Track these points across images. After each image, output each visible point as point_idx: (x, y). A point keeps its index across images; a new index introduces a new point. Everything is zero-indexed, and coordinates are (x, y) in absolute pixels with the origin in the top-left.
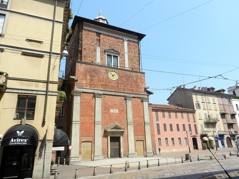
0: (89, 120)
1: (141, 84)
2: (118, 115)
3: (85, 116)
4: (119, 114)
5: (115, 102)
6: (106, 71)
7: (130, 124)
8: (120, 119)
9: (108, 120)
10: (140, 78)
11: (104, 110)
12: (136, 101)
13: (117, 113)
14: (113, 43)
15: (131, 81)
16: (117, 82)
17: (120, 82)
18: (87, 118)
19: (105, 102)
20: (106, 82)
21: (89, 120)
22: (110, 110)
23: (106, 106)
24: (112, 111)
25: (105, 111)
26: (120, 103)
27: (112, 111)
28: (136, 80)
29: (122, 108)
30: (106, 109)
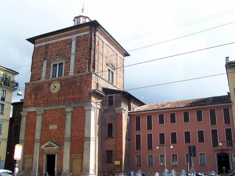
0: (31, 139)
1: (86, 88)
2: (56, 131)
3: (28, 134)
4: (57, 129)
5: (55, 117)
6: (48, 84)
7: (67, 140)
8: (58, 135)
9: (46, 137)
10: (86, 81)
11: (44, 127)
12: (78, 112)
13: (56, 129)
14: (60, 49)
15: (74, 88)
16: (59, 94)
17: (61, 93)
18: (30, 136)
19: (46, 118)
20: (47, 97)
21: (31, 139)
22: (49, 126)
23: (46, 122)
24: (51, 127)
25: (45, 129)
26: (59, 117)
27: (51, 127)
28: (80, 84)
29: (61, 123)
30: (45, 125)
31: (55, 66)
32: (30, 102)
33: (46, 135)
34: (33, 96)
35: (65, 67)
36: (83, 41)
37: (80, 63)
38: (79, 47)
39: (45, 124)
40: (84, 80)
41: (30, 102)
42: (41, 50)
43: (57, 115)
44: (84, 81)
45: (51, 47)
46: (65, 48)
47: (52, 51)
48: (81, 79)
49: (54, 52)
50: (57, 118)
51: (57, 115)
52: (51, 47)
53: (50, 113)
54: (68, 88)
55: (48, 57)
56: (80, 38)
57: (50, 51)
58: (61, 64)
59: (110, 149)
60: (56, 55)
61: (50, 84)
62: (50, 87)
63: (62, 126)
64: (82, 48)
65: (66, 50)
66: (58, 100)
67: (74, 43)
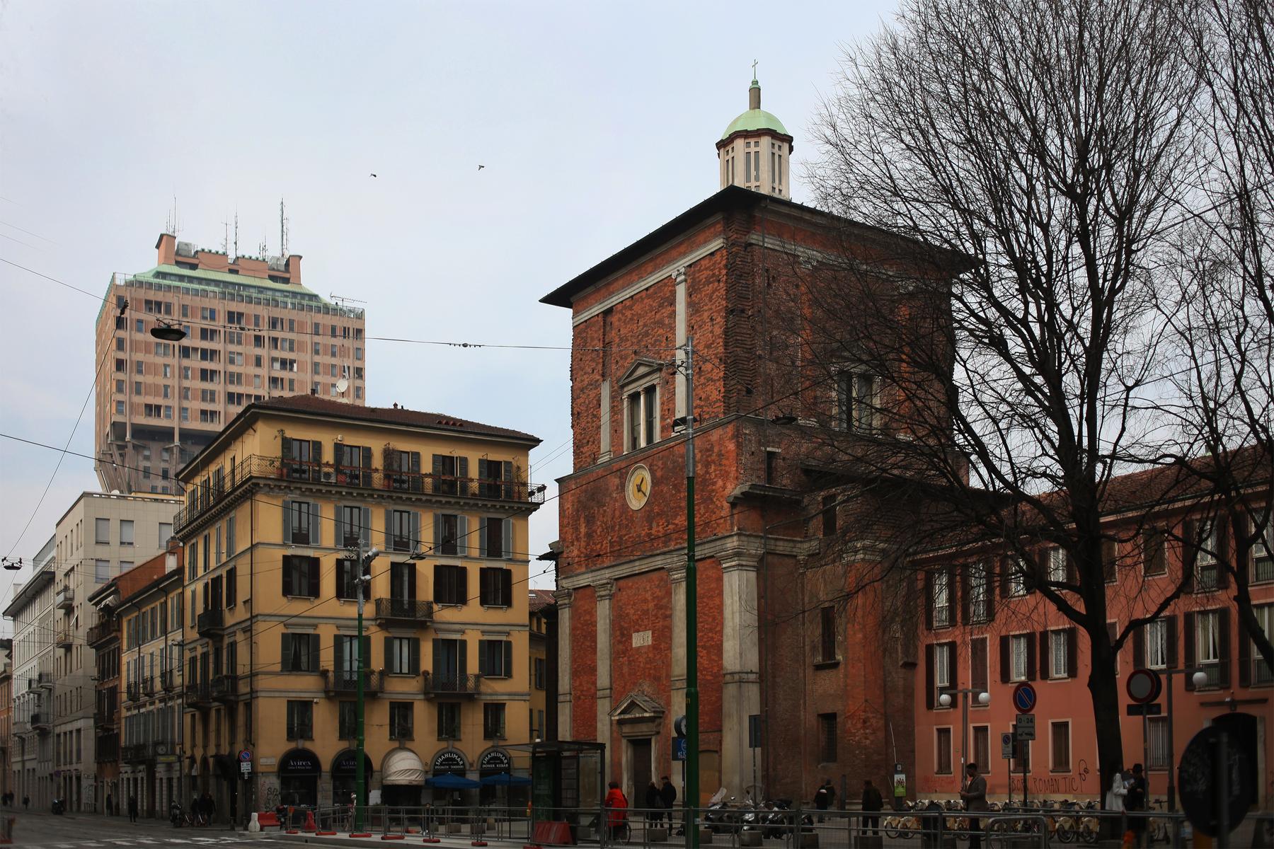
5: (645, 601)
11: (620, 642)
17: (656, 510)
25: (621, 647)
30: (621, 633)
31: (634, 398)
32: (576, 552)
33: (625, 670)
34: (583, 530)
35: (662, 404)
36: (708, 282)
37: (702, 380)
38: (697, 311)
39: (621, 628)
40: (716, 450)
41: (576, 552)
42: (592, 339)
43: (648, 596)
44: (714, 457)
45: (619, 320)
46: (658, 322)
47: (621, 339)
48: (708, 450)
49: (629, 343)
50: (651, 605)
51: (648, 596)
52: (619, 320)
53: (631, 588)
54: (675, 486)
55: (614, 367)
56: (700, 271)
57: (617, 340)
58: (650, 391)
59: (829, 709)
60: (635, 353)
61: (623, 474)
62: (622, 488)
63: (663, 636)
64: (706, 314)
65: (661, 331)
66: (649, 535)
67: (681, 291)
